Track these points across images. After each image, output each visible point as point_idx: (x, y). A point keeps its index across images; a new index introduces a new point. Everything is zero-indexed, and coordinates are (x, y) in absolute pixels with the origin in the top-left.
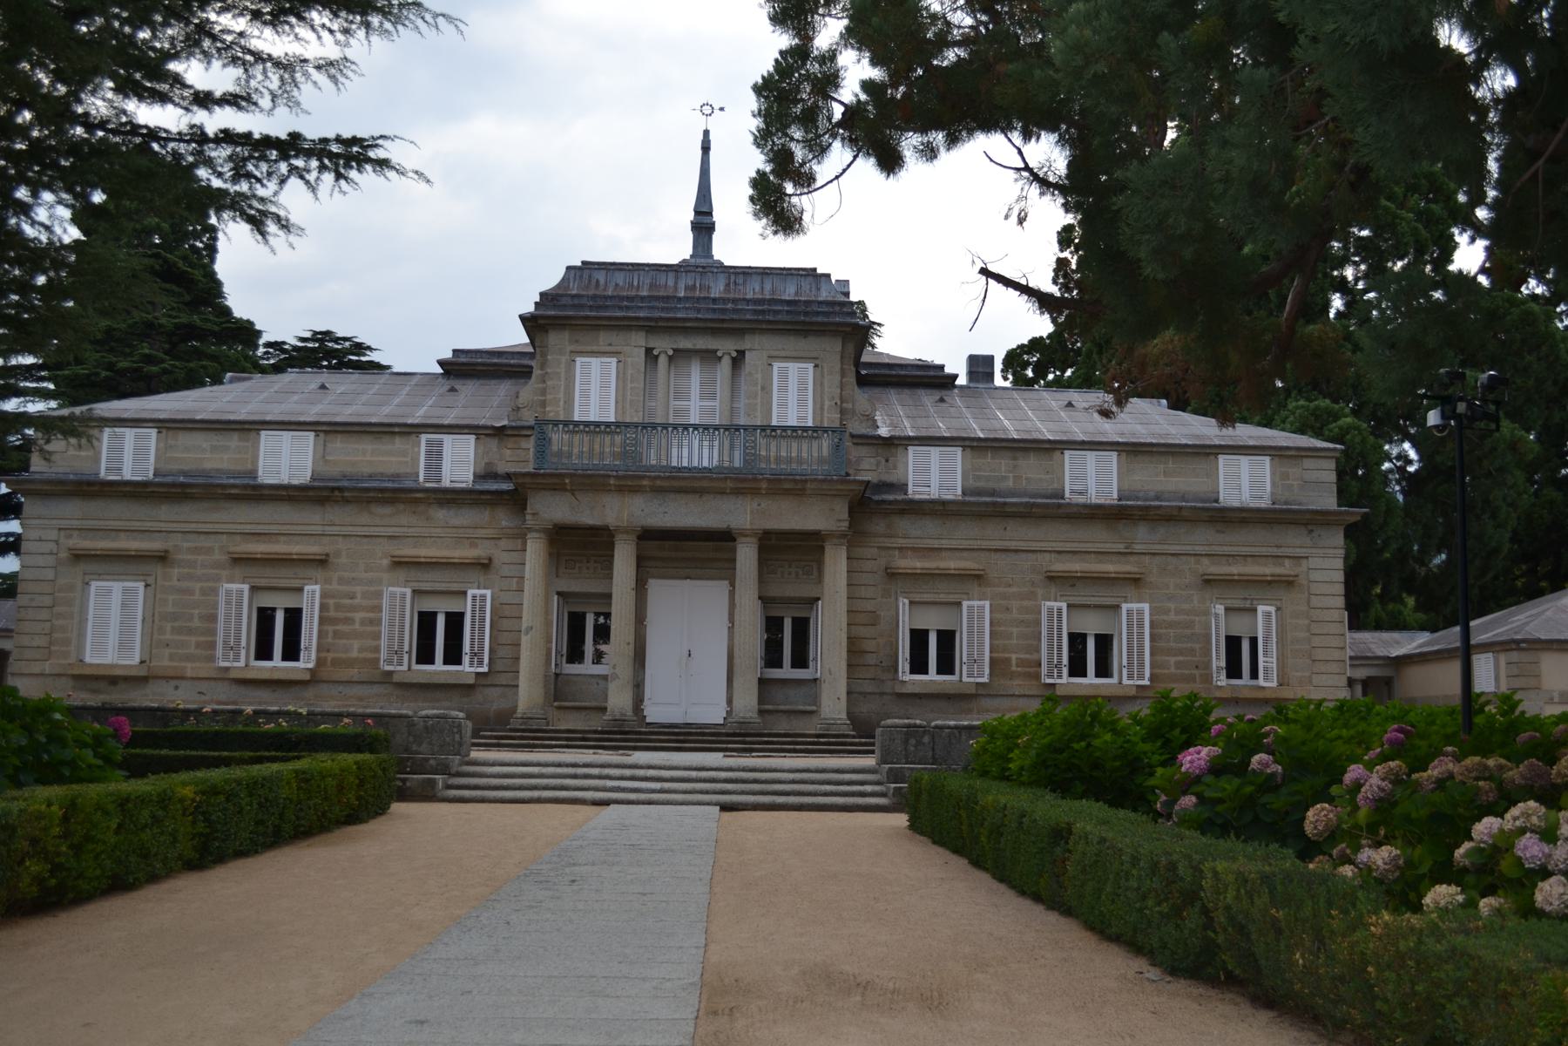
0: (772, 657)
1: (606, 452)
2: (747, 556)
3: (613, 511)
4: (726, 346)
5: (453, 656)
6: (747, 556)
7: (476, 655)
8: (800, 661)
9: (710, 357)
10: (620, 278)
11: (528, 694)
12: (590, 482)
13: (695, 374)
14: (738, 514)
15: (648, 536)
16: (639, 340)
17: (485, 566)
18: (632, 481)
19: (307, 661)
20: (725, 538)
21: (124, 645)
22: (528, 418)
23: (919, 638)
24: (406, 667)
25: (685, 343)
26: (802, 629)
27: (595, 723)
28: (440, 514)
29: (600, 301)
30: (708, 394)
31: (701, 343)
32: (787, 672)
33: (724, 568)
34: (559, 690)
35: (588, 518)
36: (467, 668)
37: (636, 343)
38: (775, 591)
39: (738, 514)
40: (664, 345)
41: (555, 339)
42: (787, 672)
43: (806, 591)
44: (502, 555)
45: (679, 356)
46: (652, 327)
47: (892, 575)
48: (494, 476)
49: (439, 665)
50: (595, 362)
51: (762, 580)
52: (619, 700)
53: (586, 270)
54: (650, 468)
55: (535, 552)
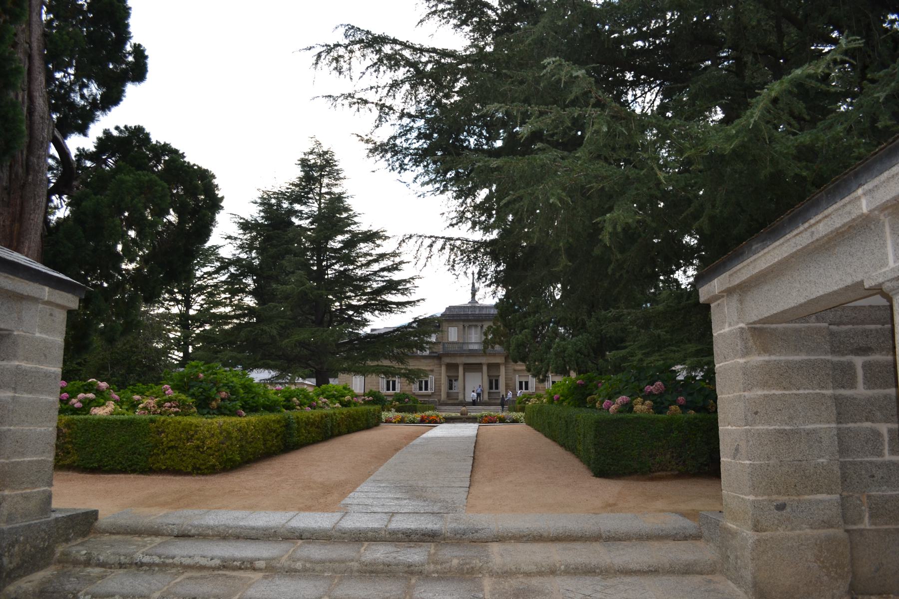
0: (491, 388)
1: (456, 347)
2: (485, 368)
3: (459, 360)
4: (479, 324)
5: (426, 389)
6: (485, 368)
7: (431, 389)
8: (497, 388)
9: (476, 326)
10: (457, 310)
11: (443, 396)
12: (454, 355)
13: (473, 330)
14: (484, 360)
15: (465, 364)
16: (462, 323)
17: (432, 371)
18: (461, 355)
19: (398, 391)
20: (481, 364)
21: (360, 389)
22: (440, 340)
23: (521, 383)
24: (418, 392)
25: (471, 324)
26: (497, 381)
27: (456, 402)
28: (423, 361)
29: (453, 316)
30: (476, 334)
31: (474, 323)
32: (494, 390)
33: (481, 371)
34: (449, 395)
35: (453, 362)
36: (429, 391)
37: (461, 325)
38: (491, 374)
39: (484, 360)
40: (467, 324)
41: (445, 324)
42: (494, 390)
43: (498, 374)
44: (436, 368)
45: (470, 327)
46: (464, 321)
47: (515, 370)
48: (433, 352)
49: (424, 391)
50: (453, 328)
51: (488, 372)
52: (461, 397)
53: (450, 309)
54: (465, 350)
55: (443, 369)
